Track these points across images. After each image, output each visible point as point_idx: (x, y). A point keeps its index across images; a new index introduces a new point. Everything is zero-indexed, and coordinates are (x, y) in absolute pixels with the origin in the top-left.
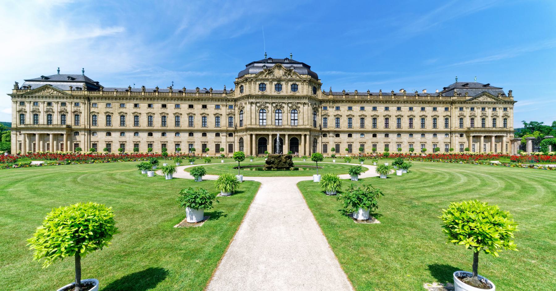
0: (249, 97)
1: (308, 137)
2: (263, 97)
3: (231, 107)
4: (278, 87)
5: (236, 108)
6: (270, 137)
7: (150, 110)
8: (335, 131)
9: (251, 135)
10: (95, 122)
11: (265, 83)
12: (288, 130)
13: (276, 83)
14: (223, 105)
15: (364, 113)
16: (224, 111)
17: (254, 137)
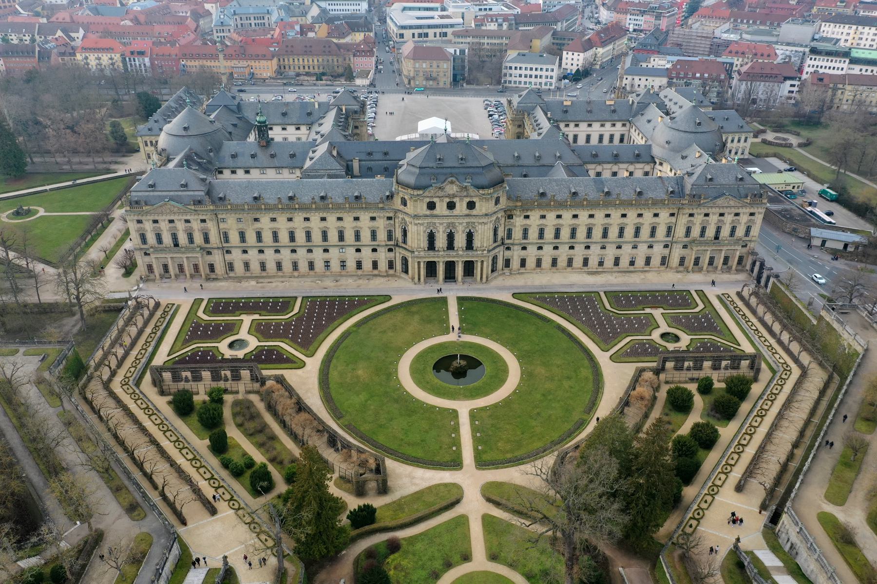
0: (416, 217)
1: (485, 263)
2: (433, 216)
3: (389, 218)
4: (451, 206)
5: (397, 220)
6: (441, 264)
7: (290, 224)
8: (520, 244)
9: (419, 263)
10: (227, 239)
11: (435, 200)
12: (462, 256)
13: (448, 200)
14: (379, 217)
15: (560, 221)
16: (381, 225)
17: (422, 264)
